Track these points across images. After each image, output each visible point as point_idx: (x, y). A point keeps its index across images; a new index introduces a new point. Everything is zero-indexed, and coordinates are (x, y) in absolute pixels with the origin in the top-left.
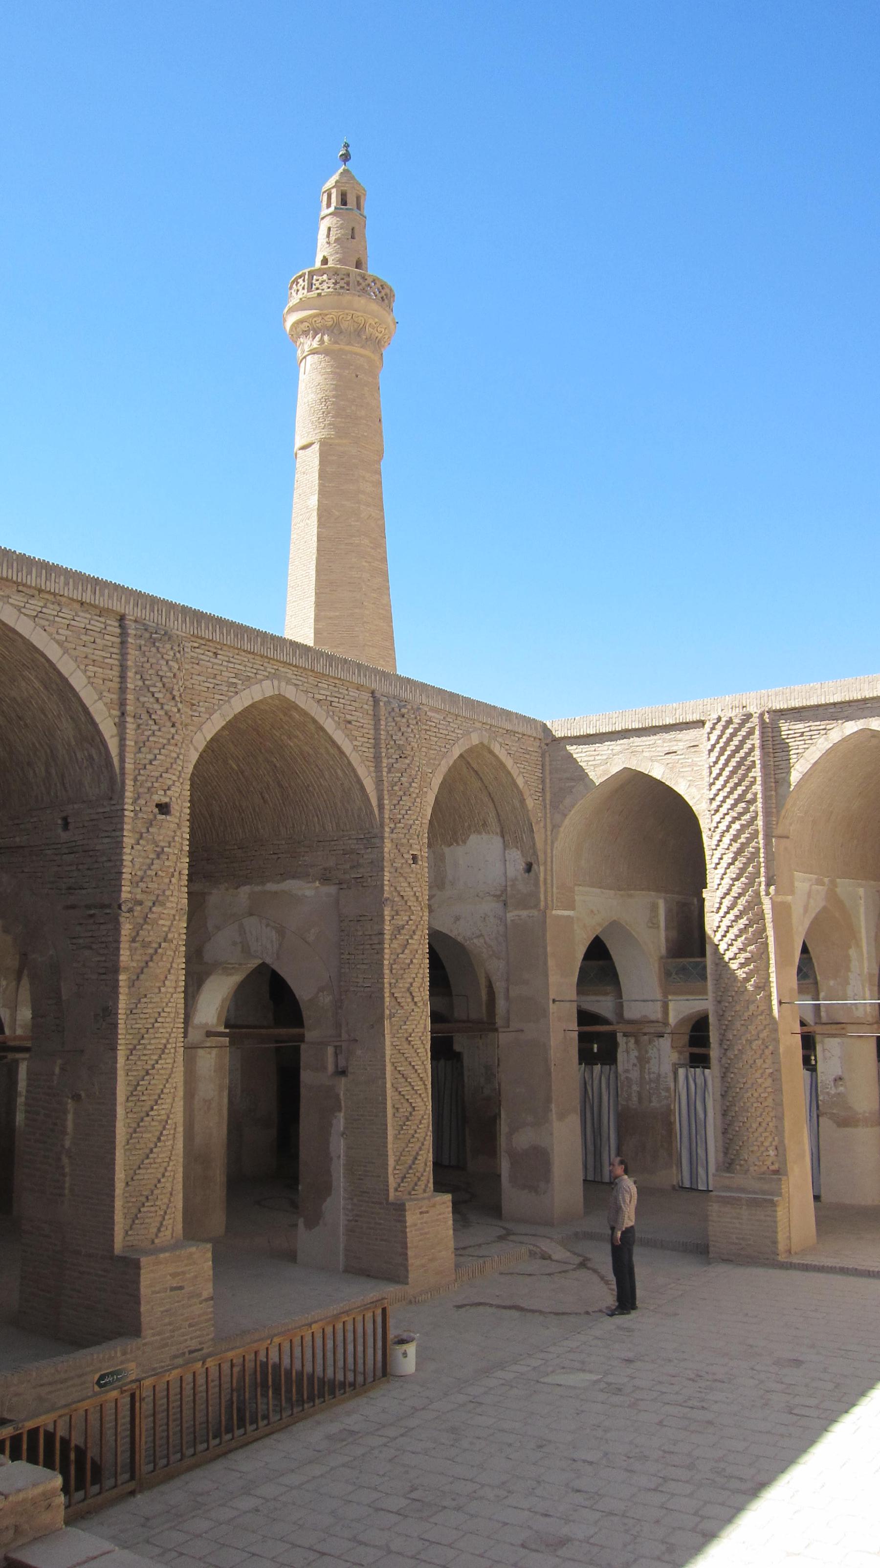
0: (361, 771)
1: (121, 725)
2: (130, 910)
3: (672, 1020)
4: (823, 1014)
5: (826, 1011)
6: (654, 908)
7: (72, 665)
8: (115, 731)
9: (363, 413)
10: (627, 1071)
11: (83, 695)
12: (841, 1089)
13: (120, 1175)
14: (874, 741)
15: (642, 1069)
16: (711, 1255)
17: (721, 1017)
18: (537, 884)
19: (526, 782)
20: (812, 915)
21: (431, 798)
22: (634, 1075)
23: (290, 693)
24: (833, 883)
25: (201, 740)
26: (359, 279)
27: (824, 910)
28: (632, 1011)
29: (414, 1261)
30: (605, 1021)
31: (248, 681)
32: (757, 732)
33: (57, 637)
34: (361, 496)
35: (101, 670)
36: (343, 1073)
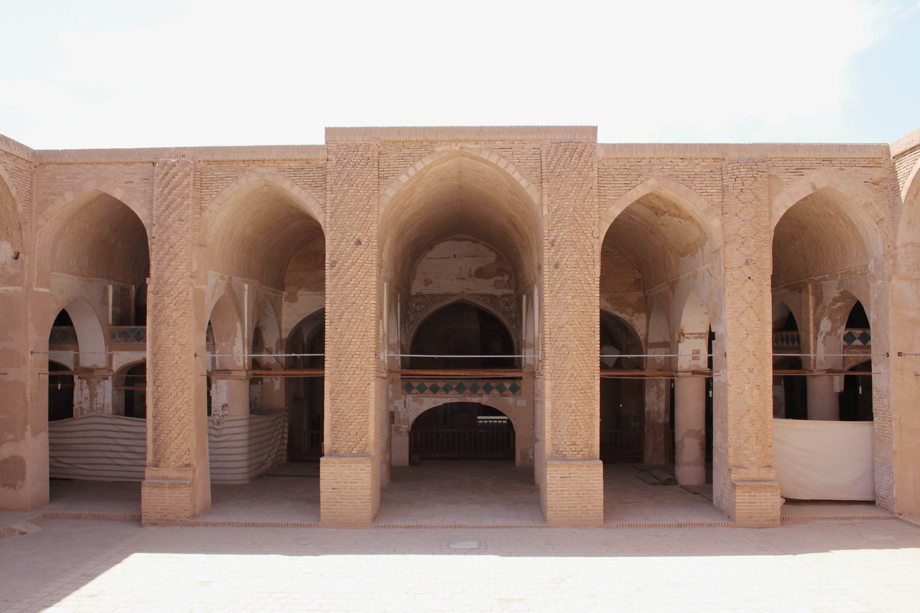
3: (116, 367)
4: (217, 364)
5: (220, 363)
6: (105, 291)
10: (81, 403)
12: (227, 412)
14: (266, 189)
15: (92, 400)
16: (143, 522)
17: (155, 365)
18: (22, 268)
19: (18, 193)
20: (216, 299)
22: (86, 405)
24: (230, 278)
27: (224, 296)
28: (87, 361)
29: (843, 380)
30: (65, 368)
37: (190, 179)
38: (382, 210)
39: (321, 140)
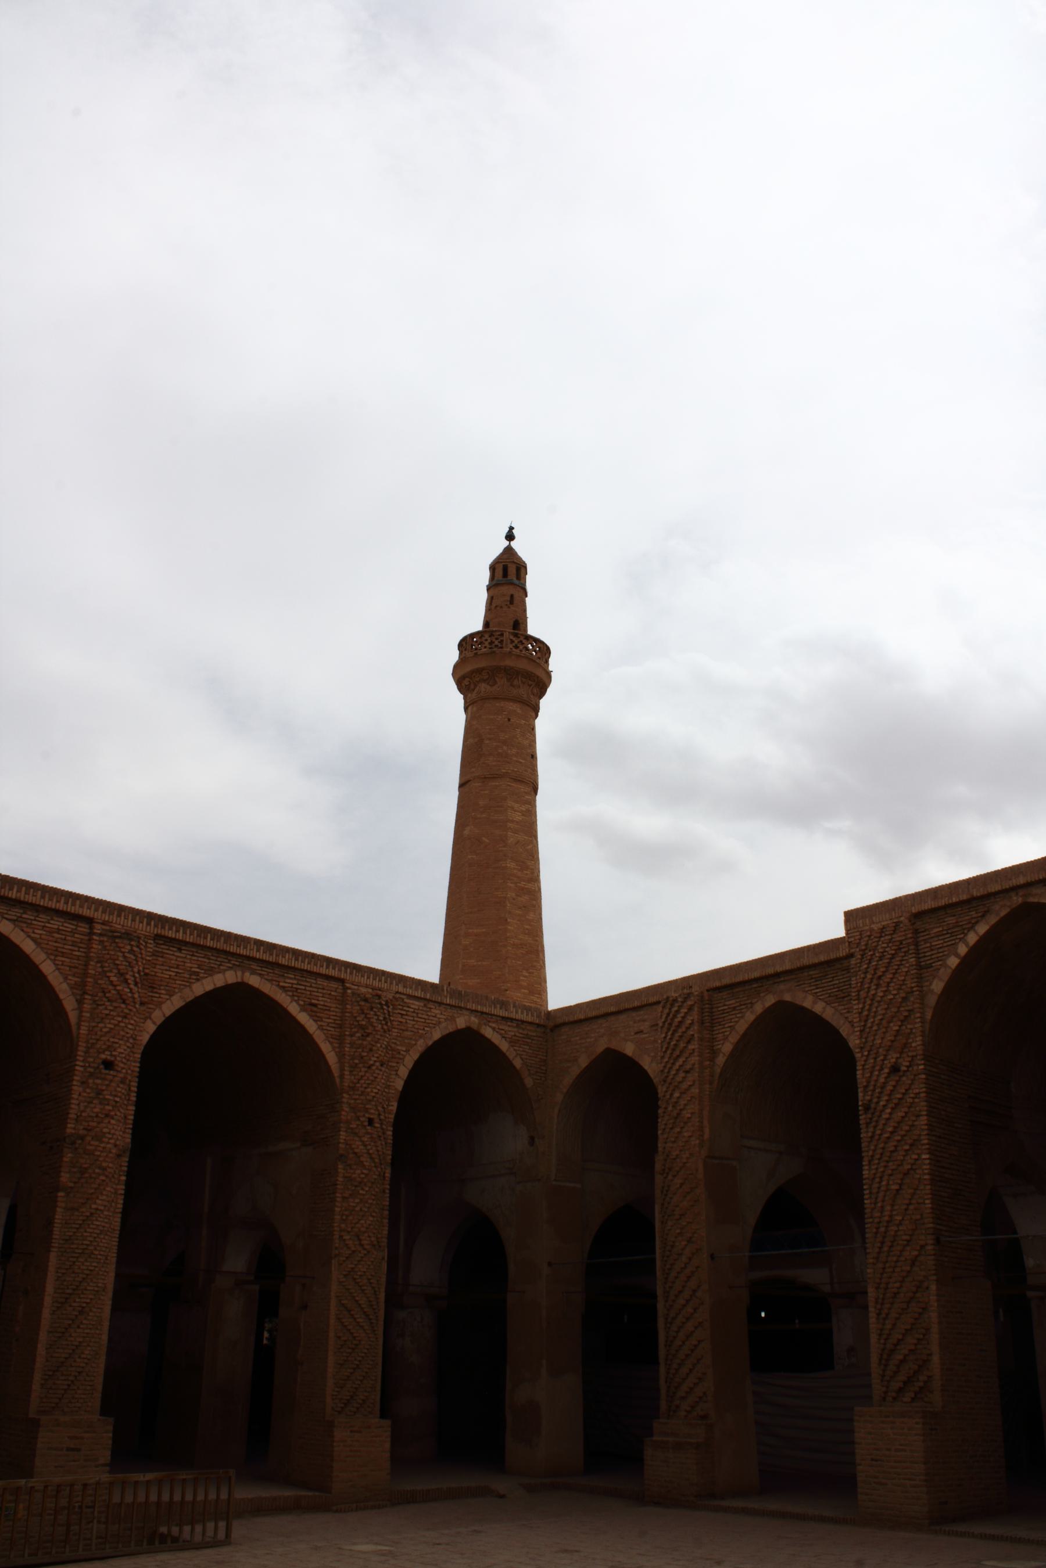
0: (325, 1047)
1: (80, 1002)
2: (73, 1143)
7: (43, 956)
8: (76, 1005)
9: (514, 751)
11: (50, 978)
13: (41, 1350)
21: (404, 1072)
23: (254, 981)
25: (159, 1016)
26: (511, 637)
31: (211, 972)
32: (696, 1009)
33: (33, 935)
34: (510, 825)
35: (68, 960)
36: (305, 1307)
37: (695, 1015)
38: (929, 1015)
39: (839, 931)
